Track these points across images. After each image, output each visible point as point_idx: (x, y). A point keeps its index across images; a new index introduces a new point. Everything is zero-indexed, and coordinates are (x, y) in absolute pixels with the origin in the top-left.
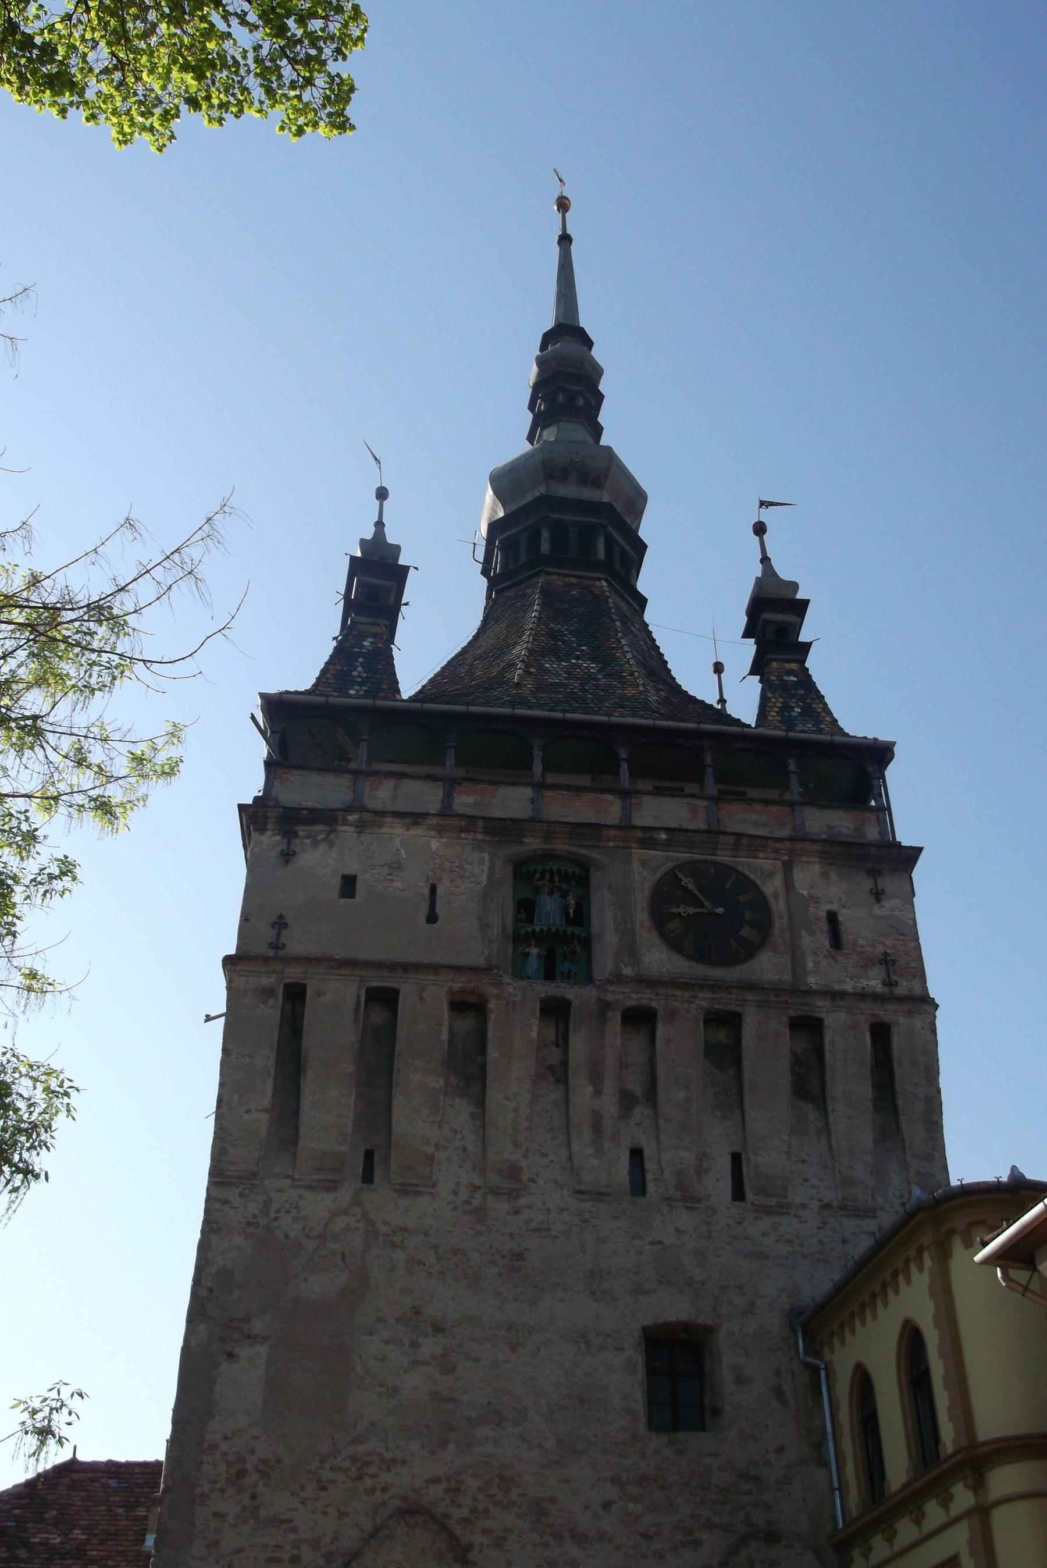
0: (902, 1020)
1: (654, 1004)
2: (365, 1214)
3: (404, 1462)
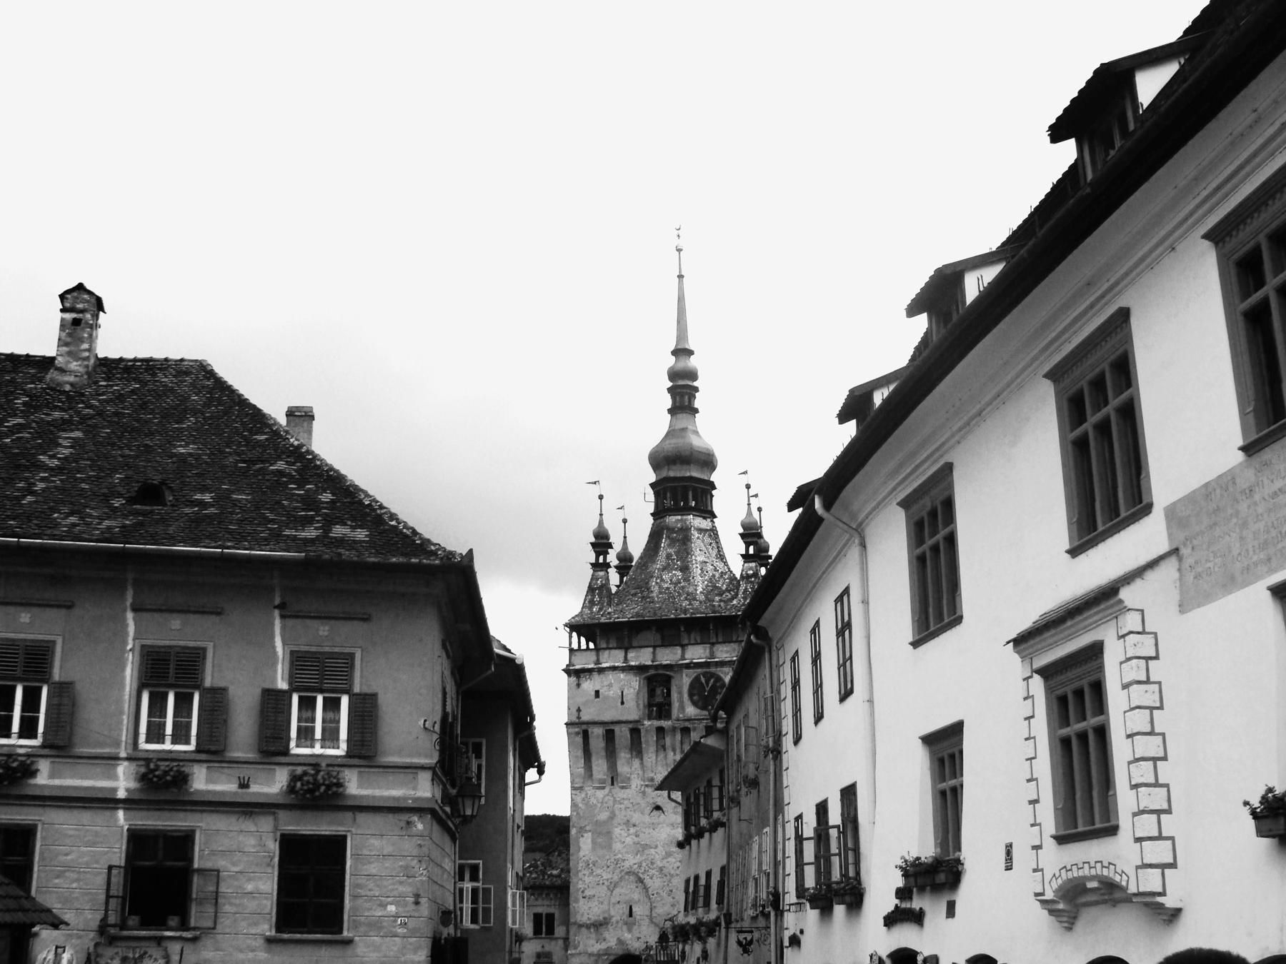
2: (613, 796)
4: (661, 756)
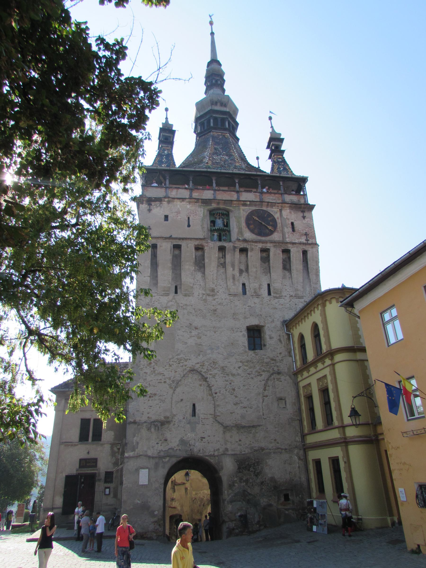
0: (310, 249)
1: (247, 247)
2: (176, 301)
3: (190, 359)
4: (222, 270)
